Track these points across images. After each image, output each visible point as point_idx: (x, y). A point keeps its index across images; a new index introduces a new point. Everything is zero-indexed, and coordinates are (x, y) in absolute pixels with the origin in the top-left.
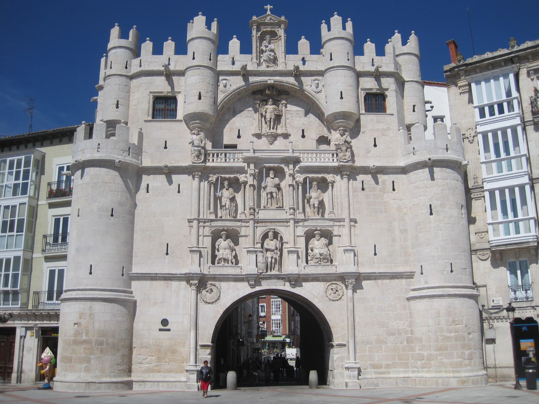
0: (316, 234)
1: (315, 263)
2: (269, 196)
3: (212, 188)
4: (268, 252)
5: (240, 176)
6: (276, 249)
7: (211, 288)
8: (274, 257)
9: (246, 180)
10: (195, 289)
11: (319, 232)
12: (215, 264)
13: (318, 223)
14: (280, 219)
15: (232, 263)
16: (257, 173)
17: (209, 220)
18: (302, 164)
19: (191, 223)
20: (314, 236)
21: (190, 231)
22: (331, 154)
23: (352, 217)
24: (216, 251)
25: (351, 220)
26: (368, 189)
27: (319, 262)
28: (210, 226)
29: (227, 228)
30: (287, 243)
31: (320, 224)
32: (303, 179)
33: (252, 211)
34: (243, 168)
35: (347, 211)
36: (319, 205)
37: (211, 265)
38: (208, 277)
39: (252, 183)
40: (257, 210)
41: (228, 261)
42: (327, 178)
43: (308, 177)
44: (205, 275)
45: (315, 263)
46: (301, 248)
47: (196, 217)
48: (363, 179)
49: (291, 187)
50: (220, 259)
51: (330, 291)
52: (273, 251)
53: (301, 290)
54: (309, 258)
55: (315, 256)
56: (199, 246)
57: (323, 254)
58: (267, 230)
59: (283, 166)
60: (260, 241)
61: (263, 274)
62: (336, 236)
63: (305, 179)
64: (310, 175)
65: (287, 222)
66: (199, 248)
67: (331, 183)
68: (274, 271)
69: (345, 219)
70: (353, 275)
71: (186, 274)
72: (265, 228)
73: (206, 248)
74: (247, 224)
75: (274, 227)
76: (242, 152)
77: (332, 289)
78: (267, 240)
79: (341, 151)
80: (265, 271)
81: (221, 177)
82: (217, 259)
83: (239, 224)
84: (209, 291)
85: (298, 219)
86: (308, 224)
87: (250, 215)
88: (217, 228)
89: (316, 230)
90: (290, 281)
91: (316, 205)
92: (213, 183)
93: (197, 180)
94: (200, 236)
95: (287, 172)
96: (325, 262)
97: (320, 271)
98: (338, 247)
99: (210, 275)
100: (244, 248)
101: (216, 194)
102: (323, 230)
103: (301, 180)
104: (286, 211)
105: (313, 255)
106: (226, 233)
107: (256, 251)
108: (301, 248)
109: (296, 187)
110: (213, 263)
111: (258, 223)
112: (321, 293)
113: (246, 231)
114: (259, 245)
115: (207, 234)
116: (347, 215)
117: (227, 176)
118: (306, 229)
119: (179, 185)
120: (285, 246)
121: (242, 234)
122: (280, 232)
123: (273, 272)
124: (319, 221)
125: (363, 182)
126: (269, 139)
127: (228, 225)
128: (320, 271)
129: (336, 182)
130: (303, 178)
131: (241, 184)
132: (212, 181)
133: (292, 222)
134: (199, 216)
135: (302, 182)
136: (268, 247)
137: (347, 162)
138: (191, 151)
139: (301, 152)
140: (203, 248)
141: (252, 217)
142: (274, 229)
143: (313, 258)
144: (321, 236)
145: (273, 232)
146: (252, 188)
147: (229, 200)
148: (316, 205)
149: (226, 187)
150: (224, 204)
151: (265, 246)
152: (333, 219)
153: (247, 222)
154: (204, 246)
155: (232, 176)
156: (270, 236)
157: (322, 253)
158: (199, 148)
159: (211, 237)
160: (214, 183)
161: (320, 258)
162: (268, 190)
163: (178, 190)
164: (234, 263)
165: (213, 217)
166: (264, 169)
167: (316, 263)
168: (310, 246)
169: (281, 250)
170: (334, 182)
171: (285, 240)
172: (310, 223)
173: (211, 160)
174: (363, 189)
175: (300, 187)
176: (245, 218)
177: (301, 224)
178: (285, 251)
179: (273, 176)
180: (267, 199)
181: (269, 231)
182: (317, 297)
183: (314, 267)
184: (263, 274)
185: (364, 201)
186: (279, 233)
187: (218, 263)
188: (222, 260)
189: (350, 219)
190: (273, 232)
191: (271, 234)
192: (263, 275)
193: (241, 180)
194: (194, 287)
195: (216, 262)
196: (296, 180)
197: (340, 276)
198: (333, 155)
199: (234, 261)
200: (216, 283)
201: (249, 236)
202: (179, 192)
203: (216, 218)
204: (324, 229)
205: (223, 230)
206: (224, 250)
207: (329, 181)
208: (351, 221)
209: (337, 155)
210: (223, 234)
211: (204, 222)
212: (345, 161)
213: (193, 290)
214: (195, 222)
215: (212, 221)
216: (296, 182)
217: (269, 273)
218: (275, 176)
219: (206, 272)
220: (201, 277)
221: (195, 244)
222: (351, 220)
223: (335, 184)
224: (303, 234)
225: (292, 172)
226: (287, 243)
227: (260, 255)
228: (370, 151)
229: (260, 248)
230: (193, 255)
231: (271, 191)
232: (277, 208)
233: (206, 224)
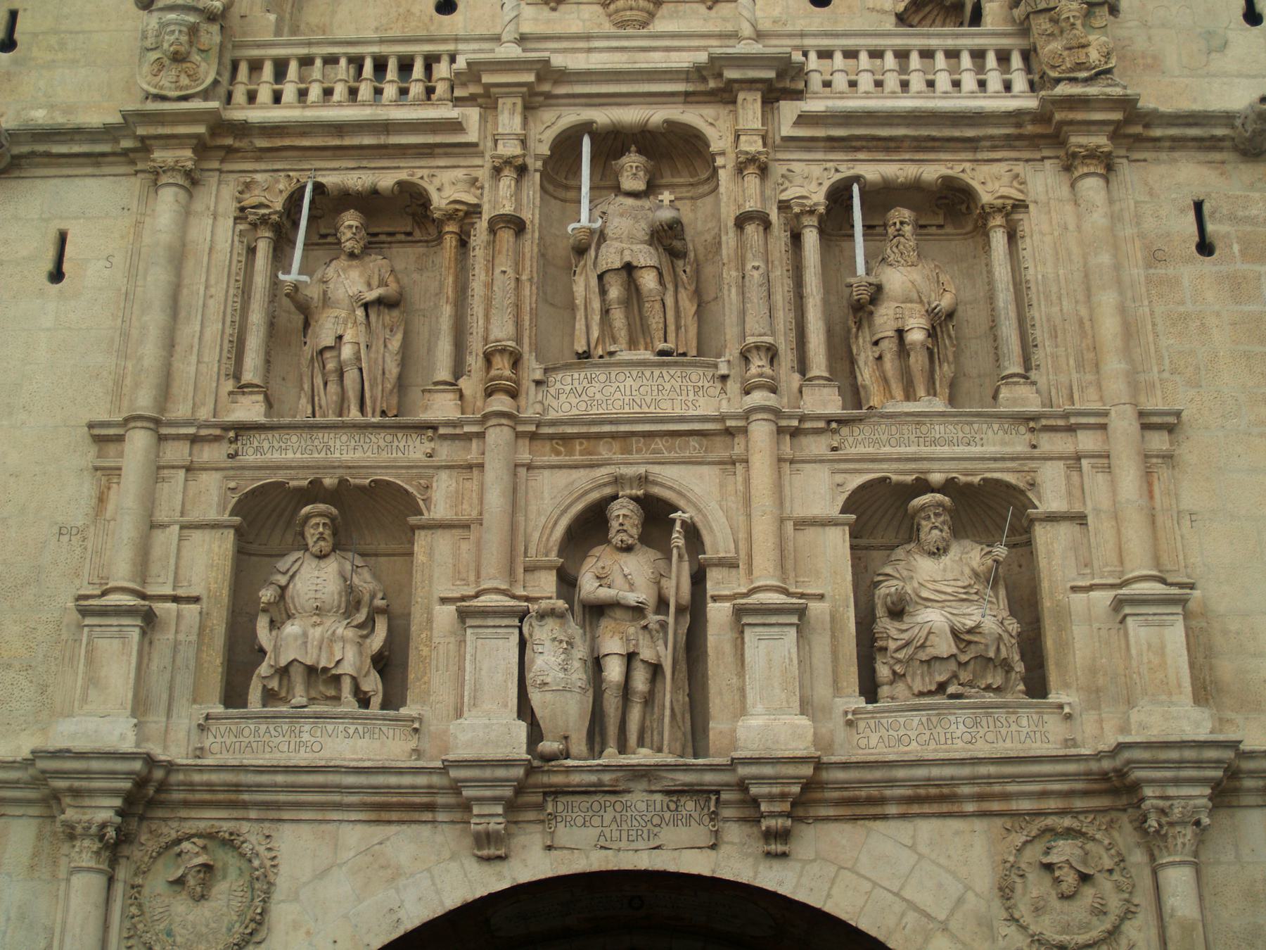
0: (923, 508)
1: (921, 694)
2: (614, 292)
3: (263, 248)
4: (606, 624)
5: (437, 182)
6: (662, 604)
7: (202, 859)
8: (646, 654)
9: (473, 200)
10: (92, 864)
11: (939, 497)
12: (245, 705)
13: (934, 442)
14: (682, 419)
15: (364, 701)
16: (539, 164)
17: (226, 428)
18: (814, 105)
19: (112, 448)
20: (910, 532)
21: (102, 499)
22: (991, 60)
23: (1154, 403)
24: (262, 624)
25: (1148, 423)
26: (1236, 248)
27: (951, 689)
28: (230, 463)
29: (343, 482)
30: (730, 564)
31: (945, 450)
32: (825, 188)
33: (502, 366)
34: (456, 126)
35: (1114, 365)
36: (932, 333)
37: (219, 709)
38: (191, 787)
39: (508, 209)
40: (533, 369)
41: (337, 679)
42: (975, 184)
43: (857, 178)
44: (170, 767)
45: (921, 694)
46: (821, 597)
47: (144, 402)
48: (1199, 193)
49: (751, 229)
50: (283, 672)
51: (1036, 886)
52: (638, 611)
53: (833, 882)
54: (883, 672)
55: (923, 646)
56: (151, 590)
57: (970, 631)
58: (600, 486)
59: (693, 116)
60: (553, 556)
61: (569, 762)
62: (1052, 518)
63: (839, 196)
64: (873, 171)
65: (729, 433)
66: (144, 597)
67: (1000, 210)
68: (644, 751)
69: (1106, 414)
70: (1199, 764)
71: (37, 754)
72: (582, 478)
73: (196, 600)
74: (472, 455)
75: (641, 470)
76: (451, 47)
77: (1049, 867)
78: (597, 551)
79: (1055, 21)
80: (579, 745)
81: (319, 188)
82: (264, 669)
83: (415, 449)
84: (191, 881)
85: (802, 418)
86: (871, 450)
87: (489, 393)
88: (279, 477)
89: (922, 486)
90: (751, 810)
91: (916, 336)
92: (264, 220)
93: (168, 199)
94: (163, 526)
95: (723, 153)
96: (988, 688)
97: (959, 744)
98: (1074, 589)
99: (201, 769)
100: (444, 601)
101: (282, 277)
102: (969, 485)
103: (818, 197)
104: (723, 370)
105: (907, 644)
106: (334, 511)
107: (523, 615)
108: (821, 597)
109: (780, 236)
110: (234, 696)
111: (533, 436)
112: (970, 895)
113: (457, 498)
114: (546, 584)
115: (212, 515)
116: (1116, 387)
117: (357, 179)
118: (856, 481)
119: (62, 238)
120: (716, 582)
121: (440, 509)
122: (681, 503)
123: (643, 756)
124: (939, 430)
125: (1198, 206)
126: (617, 11)
127: (349, 456)
128: (959, 744)
129: (1032, 207)
130: (827, 185)
131: (439, 224)
132: (266, 211)
133: (761, 431)
134: (163, 410)
135: (822, 209)
136: (604, 593)
137: (1086, 81)
138: (144, 37)
139: (808, 42)
140: (176, 599)
141: (501, 403)
142: (644, 480)
143: (911, 659)
144: (958, 531)
145: (636, 499)
146: (506, 236)
147: (360, 313)
148: (916, 336)
149: (349, 245)
150: (329, 341)
151: (589, 586)
152: (1036, 417)
153: (468, 437)
154: (181, 592)
155: (387, 180)
156: (615, 525)
157: (970, 623)
158: (191, 18)
159: (231, 534)
160: (275, 217)
161: (953, 656)
162: (611, 257)
163: (48, 265)
164: (376, 701)
165: (250, 410)
166: (586, 143)
167: (930, 693)
168: (887, 589)
169: (695, 609)
170: (1020, 206)
171: (718, 542)
172: (876, 442)
173: (265, 94)
174: (1205, 247)
175: (811, 238)
176: (455, 414)
177: (817, 446)
178: (718, 613)
179: (640, 185)
180: (606, 312)
181: (615, 497)
182: (945, 928)
183: (916, 719)
184: (569, 762)
185: (1218, 314)
186: (676, 509)
187: (270, 696)
188: (298, 676)
189: (1141, 414)
190: (636, 499)
191: (624, 514)
192: (568, 770)
193: (439, 202)
194: (85, 854)
195: (255, 694)
196: (784, 196)
197: (1104, 776)
198: (1003, 58)
199: (373, 683)
200: (245, 827)
201: (480, 523)
202: (57, 275)
203: (268, 414)
204: (976, 479)
205: (315, 492)
206: (315, 618)
207: (986, 198)
208: (1146, 427)
209: (1026, 56)
210: (308, 517)
211: (194, 440)
212: (1084, 74)
213: (79, 870)
214: (139, 440)
215: (242, 429)
216: (784, 206)
217: (611, 756)
218: (652, 188)
219: (176, 751)
220: (141, 782)
221: (121, 573)
222: (1148, 423)
223: (1033, 223)
224: (833, 509)
225: (752, 145)
226: (732, 565)
227: (543, 634)
228: (1225, 44)
229: (550, 598)
230: (102, 644)
231: (627, 258)
232: (662, 353)
233: (211, 454)
